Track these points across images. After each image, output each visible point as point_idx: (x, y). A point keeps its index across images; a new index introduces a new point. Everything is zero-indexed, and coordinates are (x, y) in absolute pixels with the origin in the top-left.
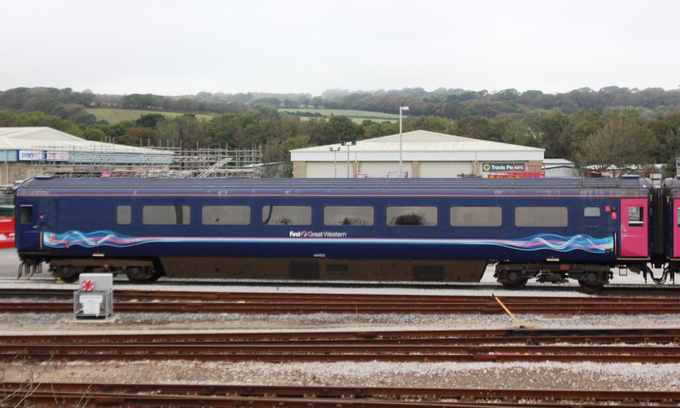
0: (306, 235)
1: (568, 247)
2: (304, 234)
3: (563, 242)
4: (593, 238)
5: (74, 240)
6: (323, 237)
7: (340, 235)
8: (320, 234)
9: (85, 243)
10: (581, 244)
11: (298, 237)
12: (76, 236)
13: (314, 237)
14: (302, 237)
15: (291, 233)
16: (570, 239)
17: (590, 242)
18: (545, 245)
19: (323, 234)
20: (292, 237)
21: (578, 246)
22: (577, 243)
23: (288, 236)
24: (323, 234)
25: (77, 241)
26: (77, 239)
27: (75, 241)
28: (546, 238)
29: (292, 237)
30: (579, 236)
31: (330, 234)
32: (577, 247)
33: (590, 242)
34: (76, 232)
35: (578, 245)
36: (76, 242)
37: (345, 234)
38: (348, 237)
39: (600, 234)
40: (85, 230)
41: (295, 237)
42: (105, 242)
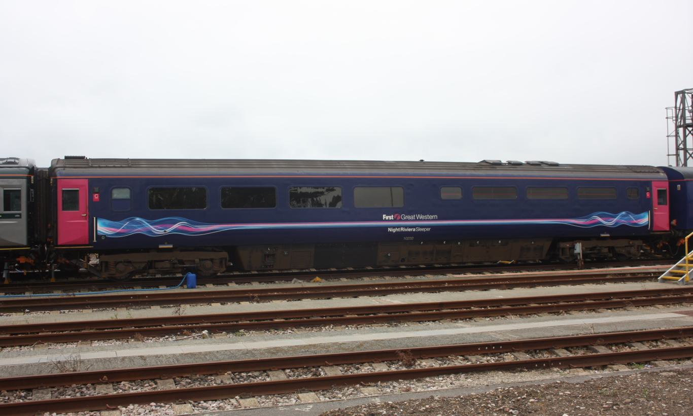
1: (616, 223)
2: (397, 216)
3: (613, 219)
4: (633, 214)
5: (136, 228)
6: (416, 220)
7: (432, 217)
8: (413, 217)
9: (150, 232)
10: (625, 220)
11: (392, 220)
13: (407, 220)
14: (395, 220)
15: (384, 216)
16: (617, 216)
17: (632, 217)
18: (600, 223)
19: (416, 217)
20: (385, 220)
21: (624, 221)
22: (623, 219)
23: (381, 220)
24: (416, 217)
25: (140, 229)
26: (139, 227)
27: (138, 230)
28: (601, 216)
29: (385, 220)
30: (624, 213)
31: (422, 217)
32: (623, 222)
33: (632, 217)
34: (138, 219)
35: (623, 221)
36: (140, 231)
37: (436, 216)
38: (439, 219)
39: (638, 211)
41: (389, 220)
42: (175, 230)
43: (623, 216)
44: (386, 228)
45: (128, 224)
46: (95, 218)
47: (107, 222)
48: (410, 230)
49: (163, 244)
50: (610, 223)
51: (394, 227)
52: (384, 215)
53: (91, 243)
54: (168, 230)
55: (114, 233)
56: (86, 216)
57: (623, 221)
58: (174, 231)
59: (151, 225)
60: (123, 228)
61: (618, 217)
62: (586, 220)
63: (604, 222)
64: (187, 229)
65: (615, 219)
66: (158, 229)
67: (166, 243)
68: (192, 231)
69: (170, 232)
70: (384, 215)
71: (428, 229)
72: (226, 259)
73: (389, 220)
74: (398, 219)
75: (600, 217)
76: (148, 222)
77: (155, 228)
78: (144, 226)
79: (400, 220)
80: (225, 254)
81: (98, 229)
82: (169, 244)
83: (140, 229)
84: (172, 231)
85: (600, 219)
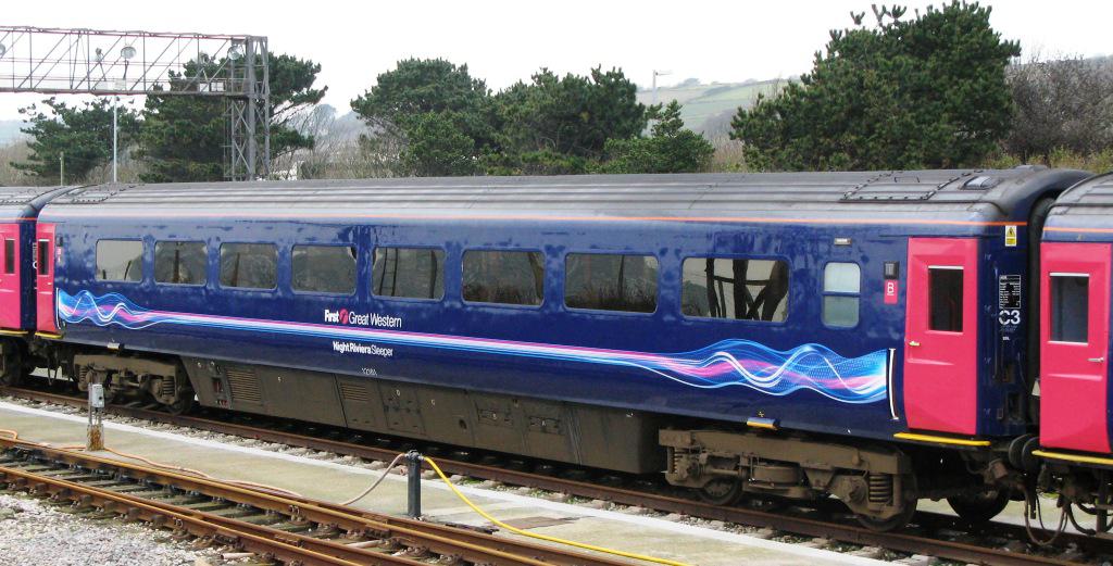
0: (345, 322)
1: (784, 384)
8: (363, 319)
14: (339, 324)
16: (788, 356)
18: (736, 376)
21: (806, 380)
23: (320, 320)
30: (807, 348)
31: (377, 320)
41: (332, 323)
43: (805, 359)
44: (329, 340)
48: (362, 350)
50: (767, 377)
51: (342, 340)
52: (327, 311)
57: (803, 376)
61: (789, 361)
63: (749, 376)
65: (781, 369)
71: (390, 352)
75: (737, 357)
79: (348, 325)
85: (736, 365)
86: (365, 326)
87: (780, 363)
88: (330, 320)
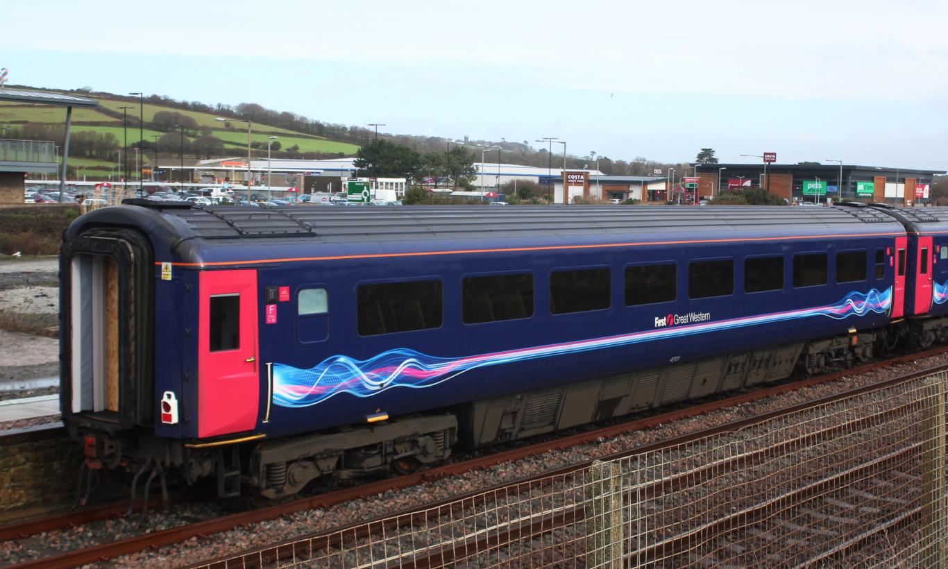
1: (865, 310)
8: (684, 319)
9: (361, 387)
11: (664, 327)
12: (344, 368)
13: (681, 325)
14: (669, 325)
15: (660, 322)
16: (866, 297)
18: (852, 310)
21: (872, 307)
23: (652, 327)
25: (345, 382)
26: (345, 377)
31: (694, 317)
34: (342, 359)
38: (713, 319)
40: (359, 353)
41: (662, 328)
45: (327, 373)
46: (269, 364)
47: (292, 371)
49: (373, 413)
50: (859, 310)
53: (260, 428)
54: (387, 381)
55: (304, 396)
56: (255, 361)
58: (396, 381)
59: (364, 370)
60: (318, 385)
61: (867, 299)
62: (841, 306)
64: (414, 373)
65: (865, 303)
66: (373, 380)
67: (379, 410)
68: (422, 379)
69: (391, 384)
70: (657, 318)
72: (452, 429)
73: (662, 328)
74: (671, 324)
76: (358, 365)
77: (369, 377)
78: (351, 374)
79: (674, 326)
80: (450, 421)
81: (274, 393)
82: (381, 413)
83: (345, 382)
84: (394, 381)
85: (852, 304)
86: (686, 324)
87: (864, 299)
88: (659, 325)
